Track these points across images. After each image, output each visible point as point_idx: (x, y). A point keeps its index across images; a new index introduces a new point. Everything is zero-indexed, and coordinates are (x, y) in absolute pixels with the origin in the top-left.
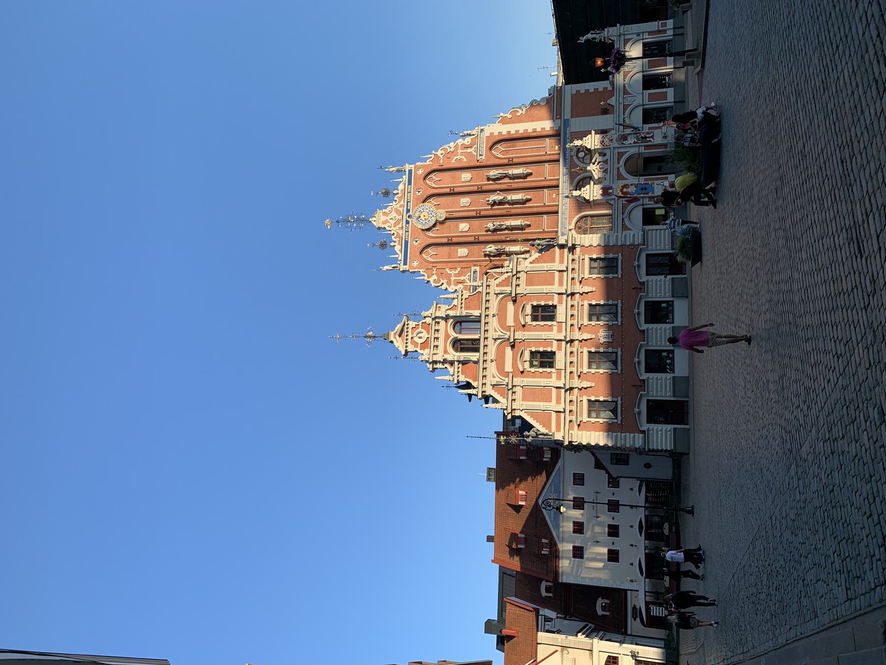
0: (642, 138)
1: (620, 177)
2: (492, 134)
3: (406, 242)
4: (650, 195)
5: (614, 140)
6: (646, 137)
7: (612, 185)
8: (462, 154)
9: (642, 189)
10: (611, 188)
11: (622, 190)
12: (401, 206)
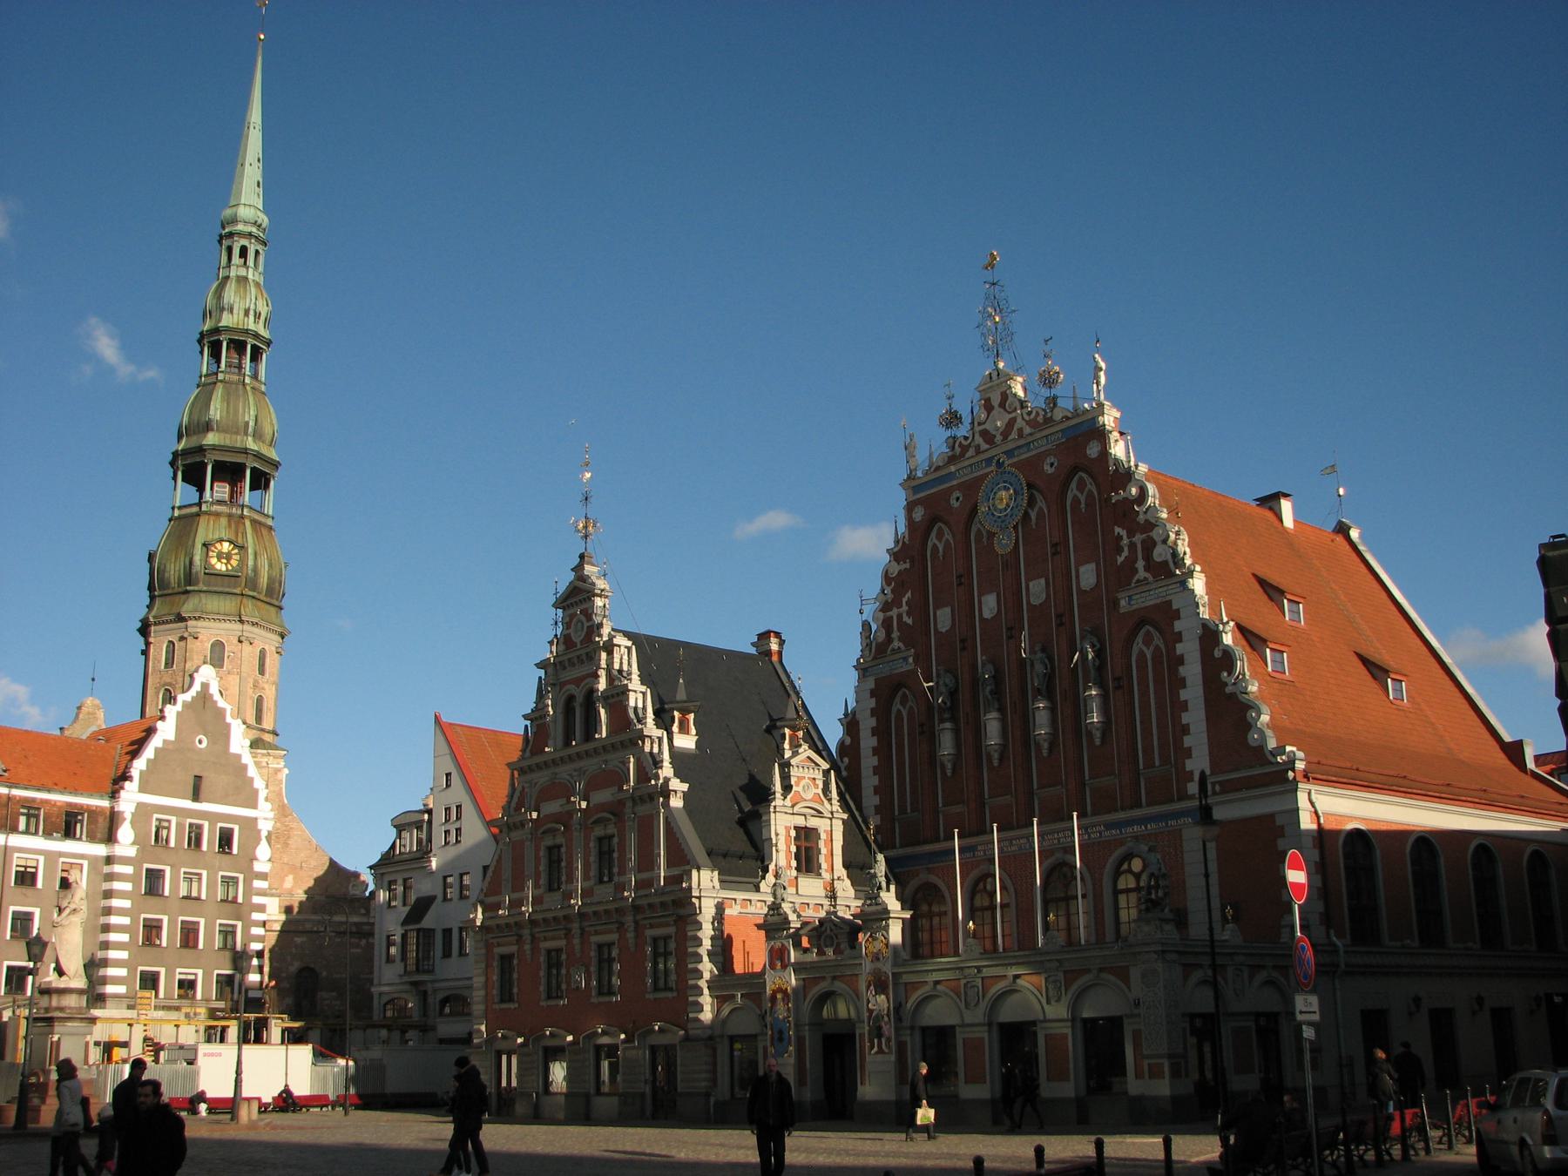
0: (880, 1028)
2: (1176, 615)
4: (771, 1050)
5: (879, 965)
6: (880, 1036)
8: (1132, 546)
11: (780, 990)
12: (1020, 430)
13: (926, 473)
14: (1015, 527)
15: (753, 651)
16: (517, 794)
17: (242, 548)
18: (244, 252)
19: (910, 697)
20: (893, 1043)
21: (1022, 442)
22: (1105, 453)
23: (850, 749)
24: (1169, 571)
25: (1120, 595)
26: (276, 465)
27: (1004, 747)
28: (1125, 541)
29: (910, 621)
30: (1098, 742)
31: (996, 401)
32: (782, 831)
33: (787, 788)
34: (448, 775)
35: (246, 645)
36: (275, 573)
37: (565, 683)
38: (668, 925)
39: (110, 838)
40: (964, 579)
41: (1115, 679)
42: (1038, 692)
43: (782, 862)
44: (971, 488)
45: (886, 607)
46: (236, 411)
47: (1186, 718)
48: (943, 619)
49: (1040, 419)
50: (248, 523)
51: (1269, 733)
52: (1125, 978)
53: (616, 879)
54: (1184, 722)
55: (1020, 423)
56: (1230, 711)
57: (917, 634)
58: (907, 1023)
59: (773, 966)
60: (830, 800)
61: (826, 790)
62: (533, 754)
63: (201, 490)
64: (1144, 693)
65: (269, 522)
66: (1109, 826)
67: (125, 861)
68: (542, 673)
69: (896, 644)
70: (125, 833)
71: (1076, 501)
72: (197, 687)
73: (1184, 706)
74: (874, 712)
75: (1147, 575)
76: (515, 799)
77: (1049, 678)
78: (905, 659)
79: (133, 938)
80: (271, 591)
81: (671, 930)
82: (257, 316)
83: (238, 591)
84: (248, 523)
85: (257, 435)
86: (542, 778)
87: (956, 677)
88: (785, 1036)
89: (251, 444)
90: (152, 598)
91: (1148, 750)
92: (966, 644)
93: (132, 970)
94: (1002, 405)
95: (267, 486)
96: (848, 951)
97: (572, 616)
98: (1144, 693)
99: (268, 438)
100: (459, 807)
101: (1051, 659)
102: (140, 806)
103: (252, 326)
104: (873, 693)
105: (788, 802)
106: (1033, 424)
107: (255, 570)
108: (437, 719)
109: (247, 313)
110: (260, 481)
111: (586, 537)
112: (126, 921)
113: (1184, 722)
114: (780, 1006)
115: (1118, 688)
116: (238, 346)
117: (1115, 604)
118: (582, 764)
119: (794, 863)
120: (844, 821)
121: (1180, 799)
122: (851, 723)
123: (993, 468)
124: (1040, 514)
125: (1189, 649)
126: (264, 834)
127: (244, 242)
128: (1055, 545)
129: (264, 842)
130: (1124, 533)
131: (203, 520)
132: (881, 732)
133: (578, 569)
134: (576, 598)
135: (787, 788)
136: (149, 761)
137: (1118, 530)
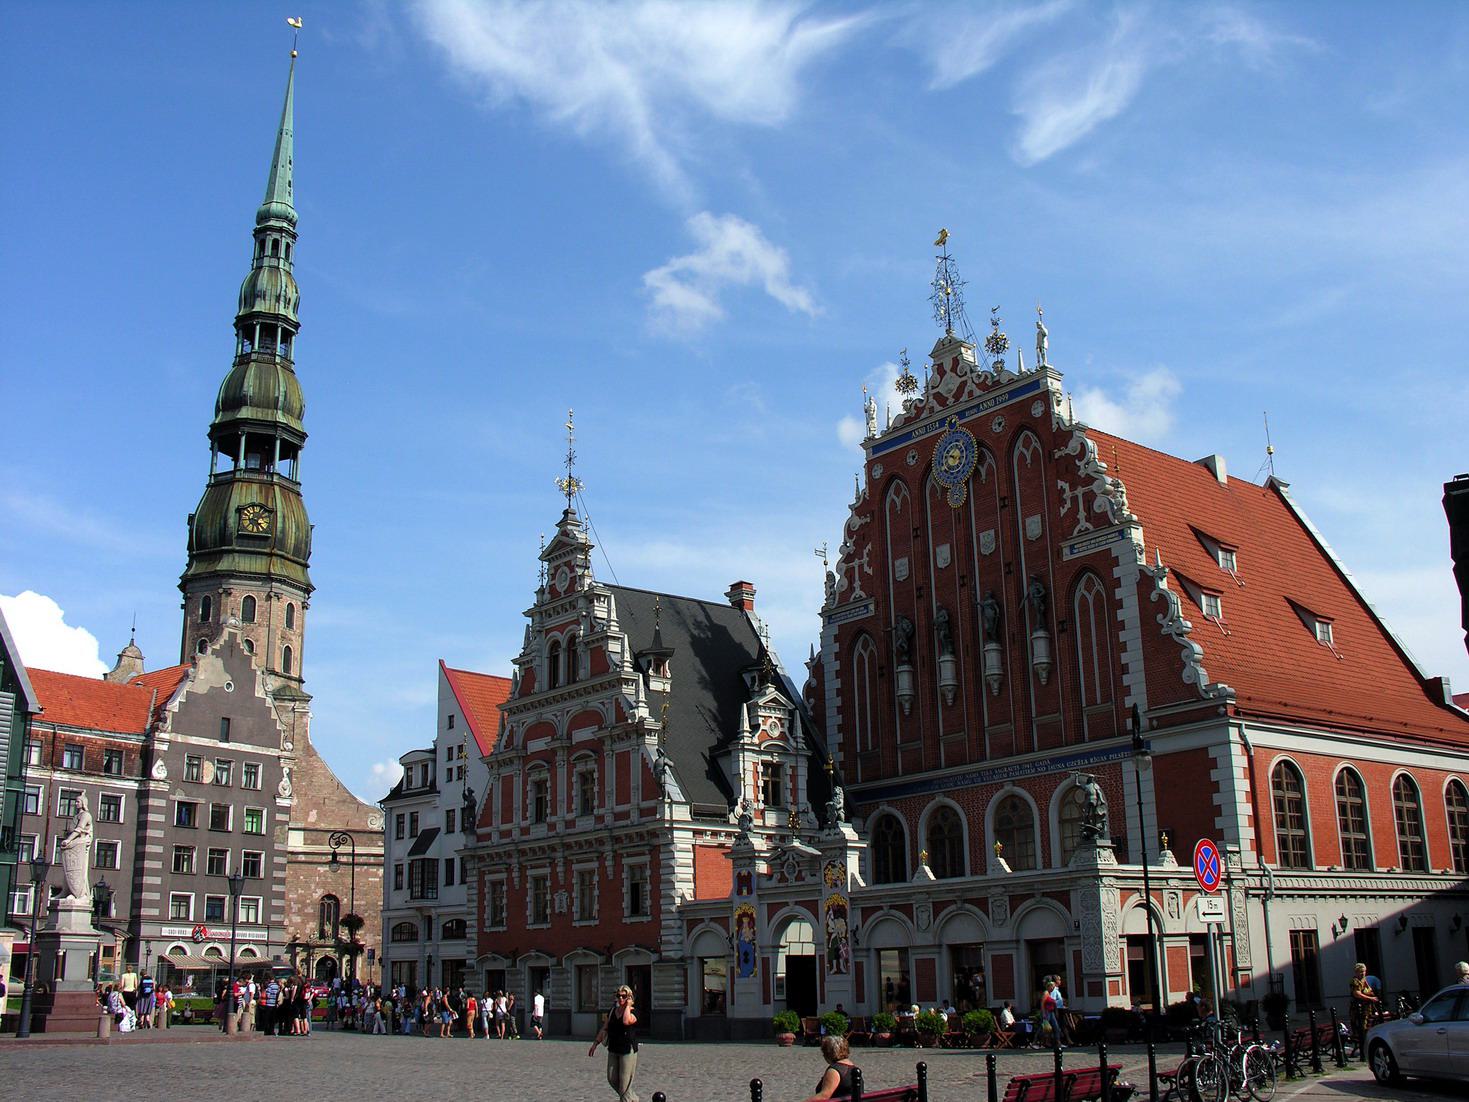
0: (838, 949)
1: (773, 909)
2: (1116, 562)
3: (908, 436)
4: (737, 970)
5: (836, 890)
6: (838, 957)
7: (754, 895)
8: (1074, 499)
9: (746, 954)
10: (750, 892)
11: (745, 914)
12: (971, 393)
13: (884, 434)
14: (967, 483)
15: (726, 602)
16: (507, 733)
17: (272, 512)
18: (276, 243)
19: (871, 642)
20: (851, 964)
21: (975, 402)
22: (1048, 412)
23: (814, 689)
24: (1107, 522)
25: (1063, 544)
26: (303, 436)
27: (958, 687)
28: (1068, 494)
29: (870, 572)
30: (1044, 681)
31: (948, 366)
32: (749, 766)
33: (755, 727)
34: (451, 717)
35: (274, 601)
36: (302, 535)
37: (548, 632)
38: (643, 854)
39: (146, 773)
40: (920, 532)
41: (1059, 623)
42: (989, 638)
43: (750, 794)
44: (926, 447)
45: (848, 558)
46: (267, 389)
47: (1125, 658)
48: (901, 568)
49: (989, 382)
50: (277, 488)
51: (1202, 671)
52: (1068, 905)
53: (595, 812)
54: (1123, 662)
55: (970, 386)
56: (1166, 651)
57: (877, 583)
58: (863, 945)
59: (740, 893)
60: (795, 738)
61: (791, 729)
62: (522, 695)
63: (236, 460)
64: (1086, 634)
65: (295, 488)
66: (1054, 761)
67: (160, 795)
68: (529, 621)
69: (858, 592)
70: (159, 771)
71: (1022, 457)
72: (225, 636)
73: (1123, 647)
74: (838, 656)
75: (1089, 525)
76: (505, 738)
77: (998, 622)
78: (866, 607)
80: (297, 550)
81: (646, 859)
82: (287, 302)
83: (267, 550)
84: (277, 488)
85: (287, 410)
86: (530, 718)
87: (913, 623)
88: (750, 957)
89: (281, 418)
90: (191, 557)
91: (1090, 689)
92: (923, 592)
94: (954, 370)
95: (295, 458)
96: (809, 879)
97: (557, 568)
98: (1086, 634)
99: (297, 412)
100: (460, 748)
101: (1001, 607)
103: (282, 311)
104: (837, 638)
105: (756, 740)
106: (983, 386)
107: (284, 528)
108: (441, 663)
109: (278, 299)
110: (291, 451)
111: (570, 494)
113: (1123, 662)
114: (746, 930)
115: (1062, 631)
116: (269, 331)
117: (1059, 553)
118: (567, 704)
119: (761, 797)
120: (809, 758)
121: (1120, 735)
122: (816, 666)
123: (946, 427)
124: (990, 472)
125: (1127, 594)
126: (286, 770)
127: (276, 236)
128: (1003, 499)
129: (286, 779)
130: (1066, 486)
131: (237, 486)
132: (844, 674)
133: (562, 524)
134: (565, 552)
135: (755, 727)
137: (1061, 483)
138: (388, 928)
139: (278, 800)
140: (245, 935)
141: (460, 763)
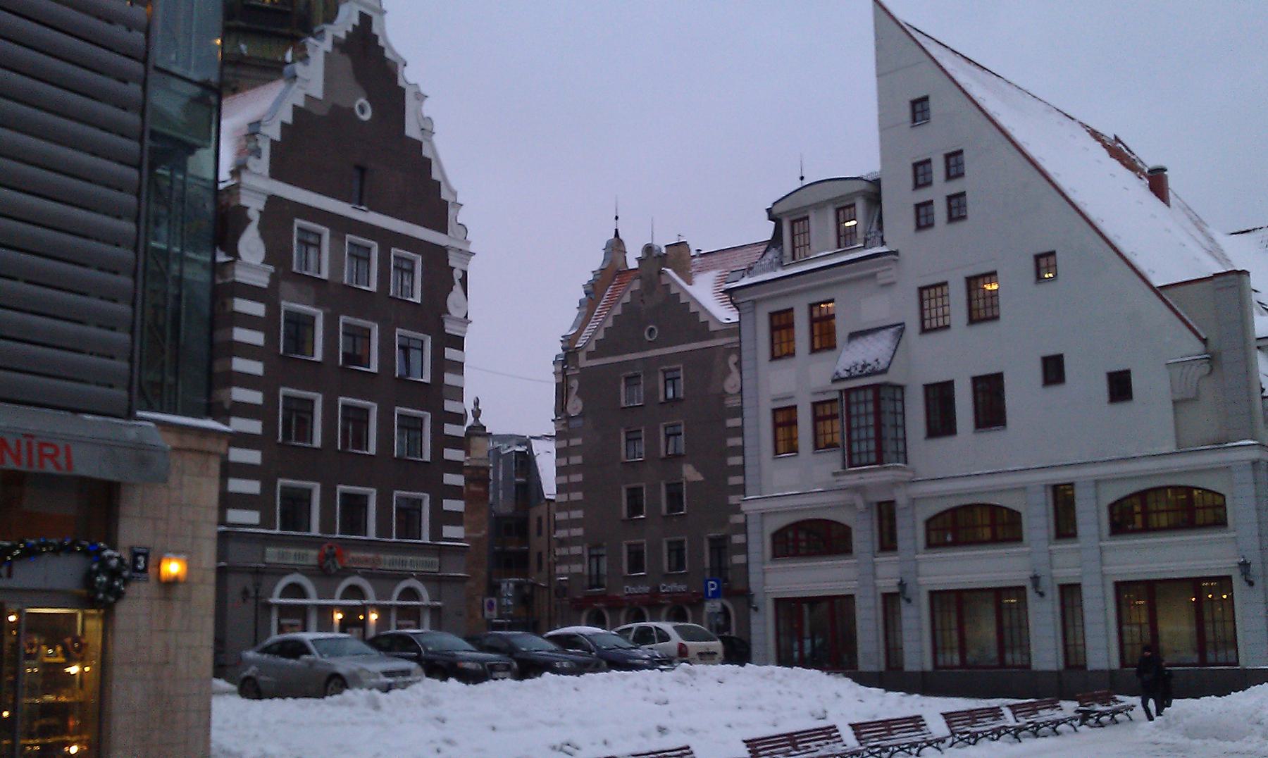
67: (252, 293)
70: (251, 246)
79: (269, 426)
83: (287, 31)
93: (268, 486)
102: (274, 201)
112: (256, 397)
129: (457, 288)
136: (284, 125)
138: (762, 533)
139: (447, 325)
140: (403, 563)
141: (955, 187)
